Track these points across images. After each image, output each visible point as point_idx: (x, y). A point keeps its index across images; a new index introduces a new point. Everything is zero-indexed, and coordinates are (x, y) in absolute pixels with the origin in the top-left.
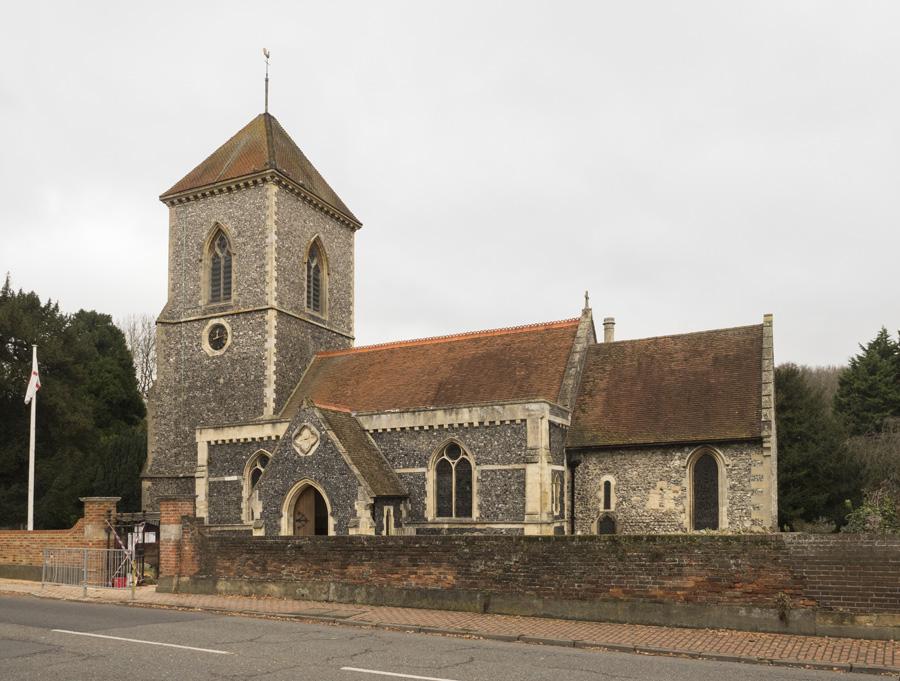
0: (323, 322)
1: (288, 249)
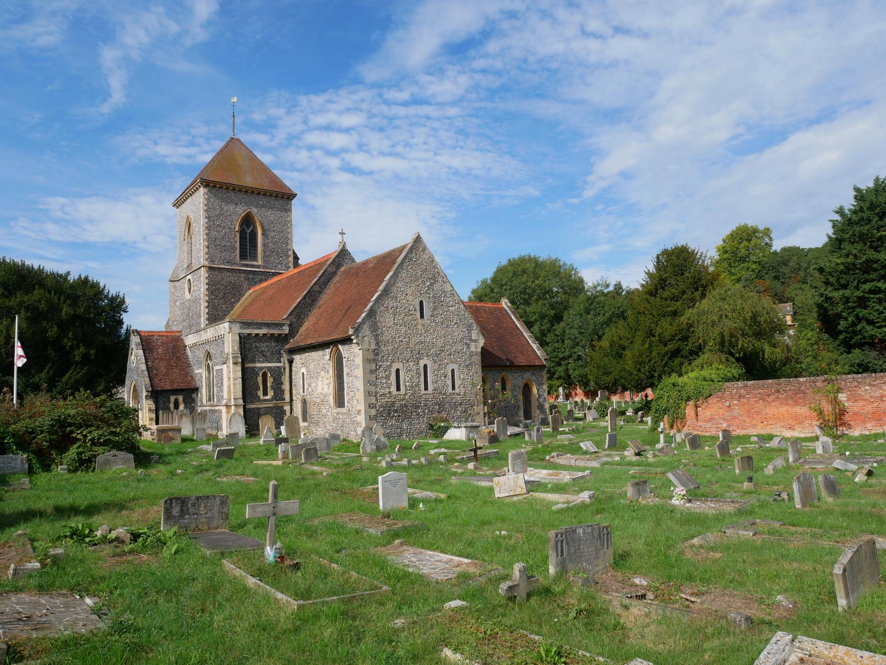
0: (258, 267)
1: (219, 226)
